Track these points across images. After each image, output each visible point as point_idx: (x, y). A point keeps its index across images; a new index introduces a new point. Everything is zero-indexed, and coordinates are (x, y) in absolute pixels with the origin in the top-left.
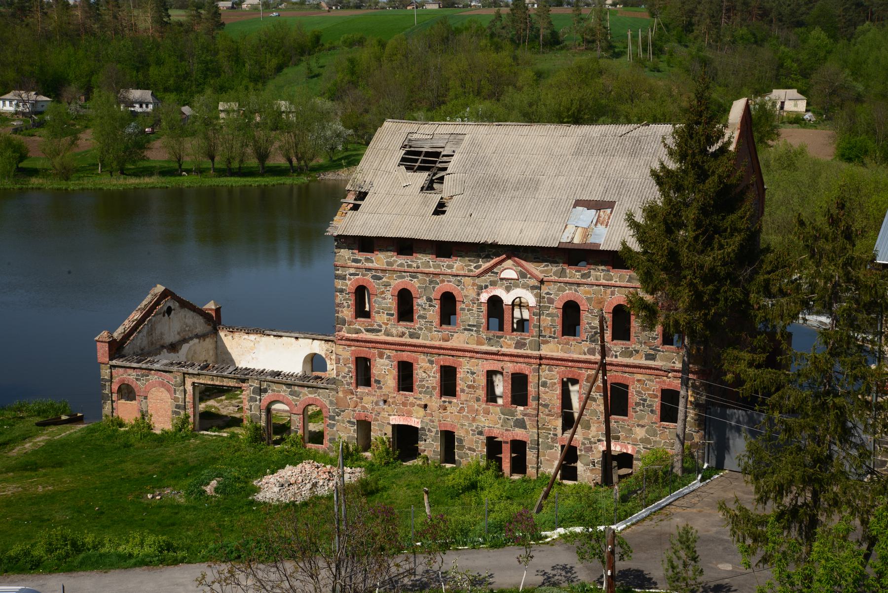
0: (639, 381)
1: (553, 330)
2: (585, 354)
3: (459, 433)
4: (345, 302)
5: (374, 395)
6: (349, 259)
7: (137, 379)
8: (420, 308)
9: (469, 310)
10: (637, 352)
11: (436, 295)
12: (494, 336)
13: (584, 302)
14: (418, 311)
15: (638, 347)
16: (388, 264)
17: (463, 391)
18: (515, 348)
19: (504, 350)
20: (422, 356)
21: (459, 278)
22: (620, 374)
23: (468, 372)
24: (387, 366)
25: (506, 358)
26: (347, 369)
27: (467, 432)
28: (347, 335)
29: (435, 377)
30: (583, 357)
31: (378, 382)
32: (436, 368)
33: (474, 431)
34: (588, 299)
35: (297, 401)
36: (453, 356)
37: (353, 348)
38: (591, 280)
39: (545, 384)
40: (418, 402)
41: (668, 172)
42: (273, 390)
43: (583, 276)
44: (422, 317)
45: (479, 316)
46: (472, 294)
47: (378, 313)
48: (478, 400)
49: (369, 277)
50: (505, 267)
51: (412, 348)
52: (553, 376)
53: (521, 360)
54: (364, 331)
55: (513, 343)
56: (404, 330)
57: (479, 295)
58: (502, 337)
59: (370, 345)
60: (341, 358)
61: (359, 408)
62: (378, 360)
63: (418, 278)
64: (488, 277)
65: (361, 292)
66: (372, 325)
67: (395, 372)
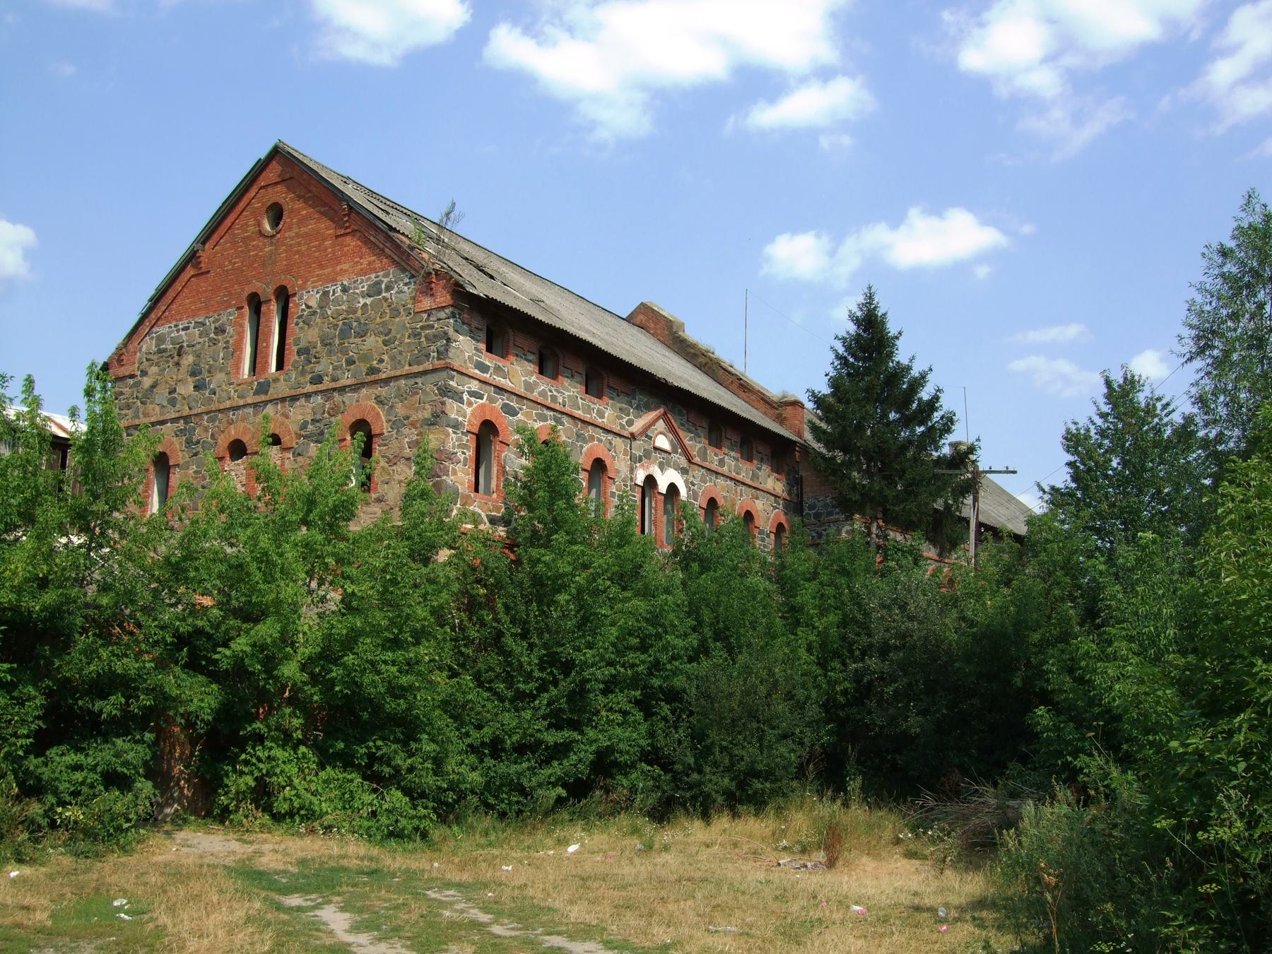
6: (470, 358)
16: (530, 387)
57: (632, 470)
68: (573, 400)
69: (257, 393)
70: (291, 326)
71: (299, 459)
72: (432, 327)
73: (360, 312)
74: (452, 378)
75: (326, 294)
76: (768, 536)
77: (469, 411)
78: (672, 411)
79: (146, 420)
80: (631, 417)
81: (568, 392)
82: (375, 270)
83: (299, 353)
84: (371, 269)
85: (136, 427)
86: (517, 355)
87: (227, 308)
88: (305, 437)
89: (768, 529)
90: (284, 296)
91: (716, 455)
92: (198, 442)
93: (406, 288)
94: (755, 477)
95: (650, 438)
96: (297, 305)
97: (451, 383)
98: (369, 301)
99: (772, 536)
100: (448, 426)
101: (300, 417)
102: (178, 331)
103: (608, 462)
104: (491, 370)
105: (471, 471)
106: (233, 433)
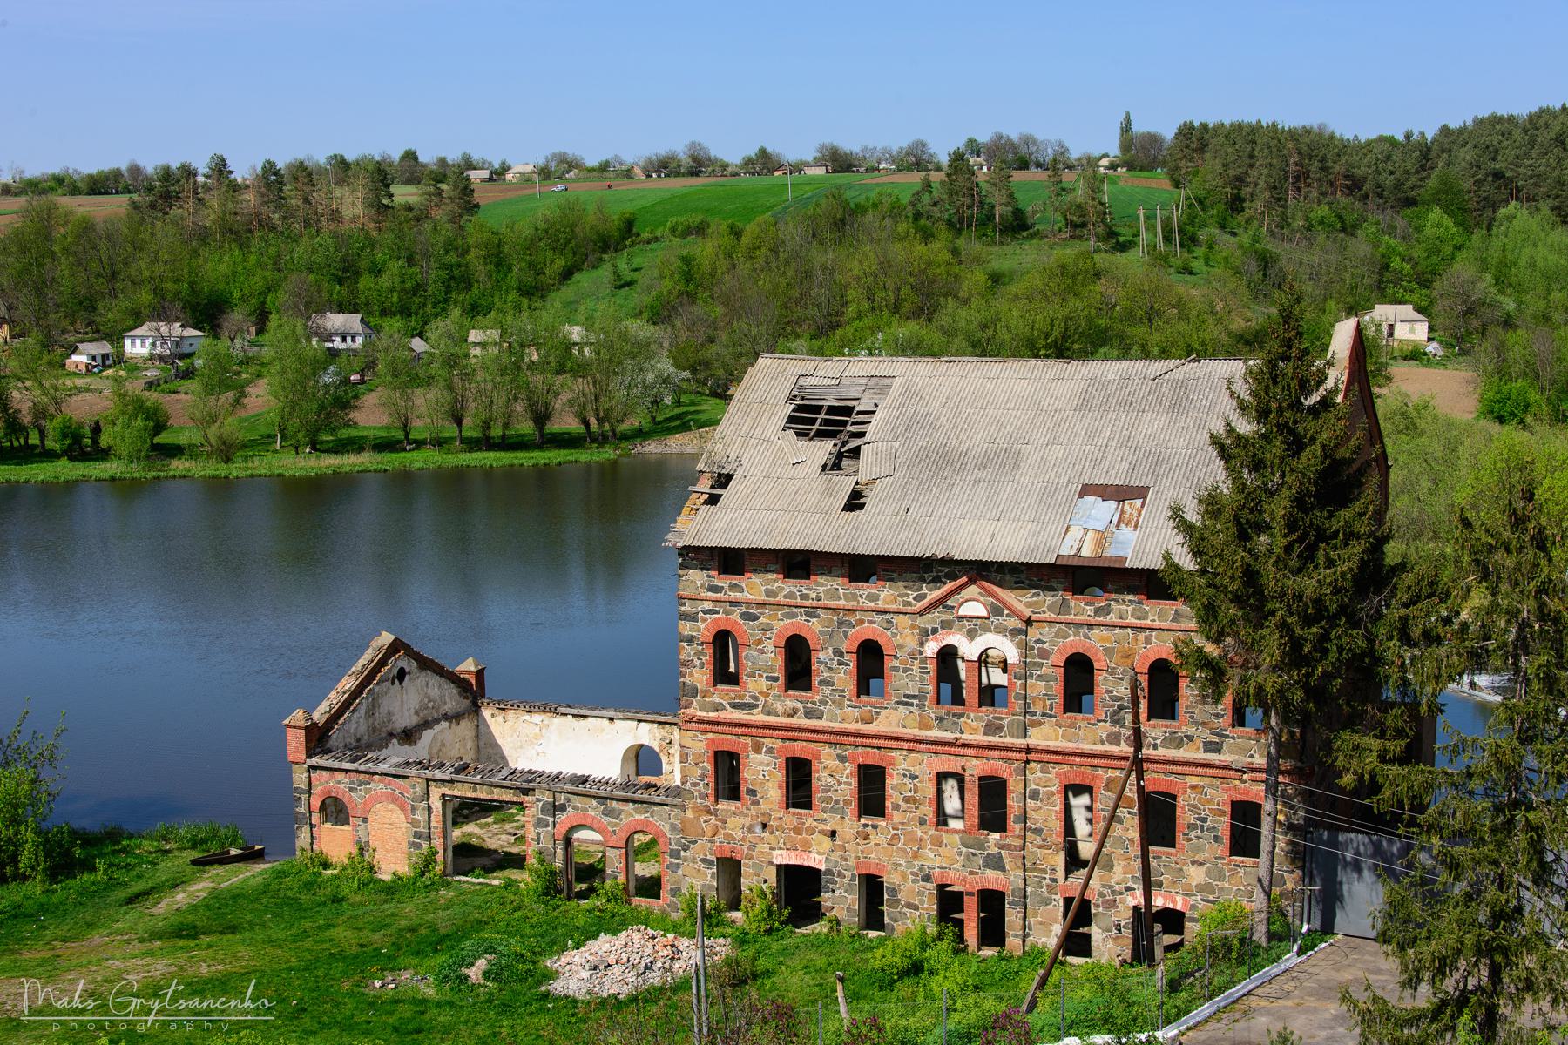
0: (1193, 787)
1: (1048, 702)
2: (1103, 743)
3: (890, 879)
4: (695, 658)
5: (746, 815)
6: (702, 586)
7: (351, 790)
8: (822, 667)
9: (905, 671)
10: (1190, 738)
11: (849, 645)
12: (948, 714)
13: (1101, 655)
14: (819, 672)
15: (1191, 731)
16: (769, 593)
17: (896, 807)
18: (985, 734)
19: (967, 737)
20: (827, 749)
21: (888, 617)
22: (1161, 776)
23: (905, 775)
24: (767, 765)
25: (970, 751)
26: (699, 772)
27: (904, 876)
28: (699, 713)
29: (850, 784)
30: (1099, 748)
31: (752, 792)
32: (850, 768)
33: (917, 875)
34: (1106, 650)
35: (616, 825)
36: (879, 748)
37: (710, 736)
38: (1112, 618)
39: (1035, 795)
40: (821, 827)
41: (1240, 439)
42: (575, 808)
43: (1098, 611)
44: (823, 682)
45: (922, 680)
46: (909, 641)
47: (752, 676)
48: (922, 822)
49: (736, 616)
50: (967, 597)
51: (810, 735)
52: (1047, 780)
53: (996, 754)
54: (728, 706)
55: (980, 725)
56: (795, 704)
57: (922, 644)
58: (961, 715)
59: (739, 730)
60: (690, 752)
61: (719, 838)
62: (752, 755)
63: (818, 616)
64: (938, 615)
65: (722, 641)
66: (742, 697)
67: (781, 776)
86: (755, 571)
95: (953, 608)
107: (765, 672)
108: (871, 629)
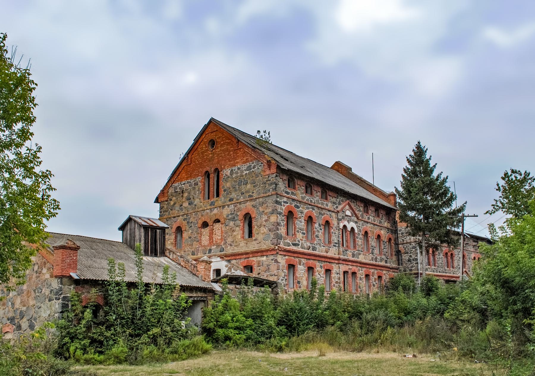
0: (384, 274)
4: (281, 222)
6: (283, 190)
17: (334, 285)
24: (303, 270)
29: (323, 277)
30: (372, 262)
32: (323, 271)
34: (370, 230)
36: (330, 262)
37: (287, 257)
45: (338, 237)
49: (293, 205)
55: (351, 254)
57: (338, 224)
59: (296, 255)
60: (281, 265)
62: (299, 266)
63: (314, 210)
66: (295, 241)
68: (318, 201)
69: (211, 205)
70: (221, 182)
71: (227, 227)
72: (270, 180)
73: (244, 176)
74: (278, 198)
75: (232, 170)
76: (386, 243)
77: (284, 208)
78: (351, 201)
79: (173, 216)
80: (337, 205)
81: (316, 198)
82: (249, 162)
83: (225, 191)
84: (247, 161)
85: (170, 218)
87: (198, 177)
88: (229, 219)
89: (386, 241)
90: (217, 172)
91: (367, 216)
92: (192, 222)
93: (260, 167)
94: (380, 222)
95: (344, 212)
96: (222, 175)
97: (278, 199)
98: (247, 172)
99: (387, 243)
100: (277, 214)
101: (226, 213)
102: (181, 185)
103: (330, 222)
104: (290, 194)
105: (285, 228)
106: (204, 219)
107: (302, 230)
108: (327, 216)
